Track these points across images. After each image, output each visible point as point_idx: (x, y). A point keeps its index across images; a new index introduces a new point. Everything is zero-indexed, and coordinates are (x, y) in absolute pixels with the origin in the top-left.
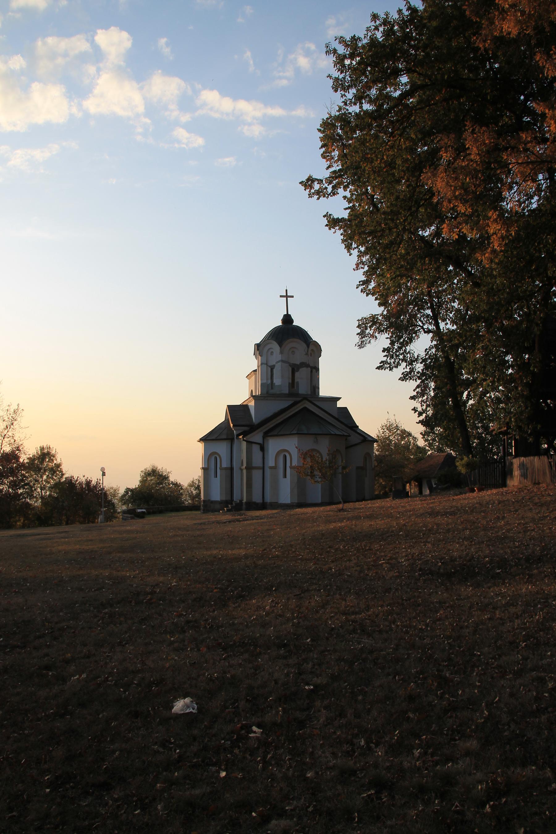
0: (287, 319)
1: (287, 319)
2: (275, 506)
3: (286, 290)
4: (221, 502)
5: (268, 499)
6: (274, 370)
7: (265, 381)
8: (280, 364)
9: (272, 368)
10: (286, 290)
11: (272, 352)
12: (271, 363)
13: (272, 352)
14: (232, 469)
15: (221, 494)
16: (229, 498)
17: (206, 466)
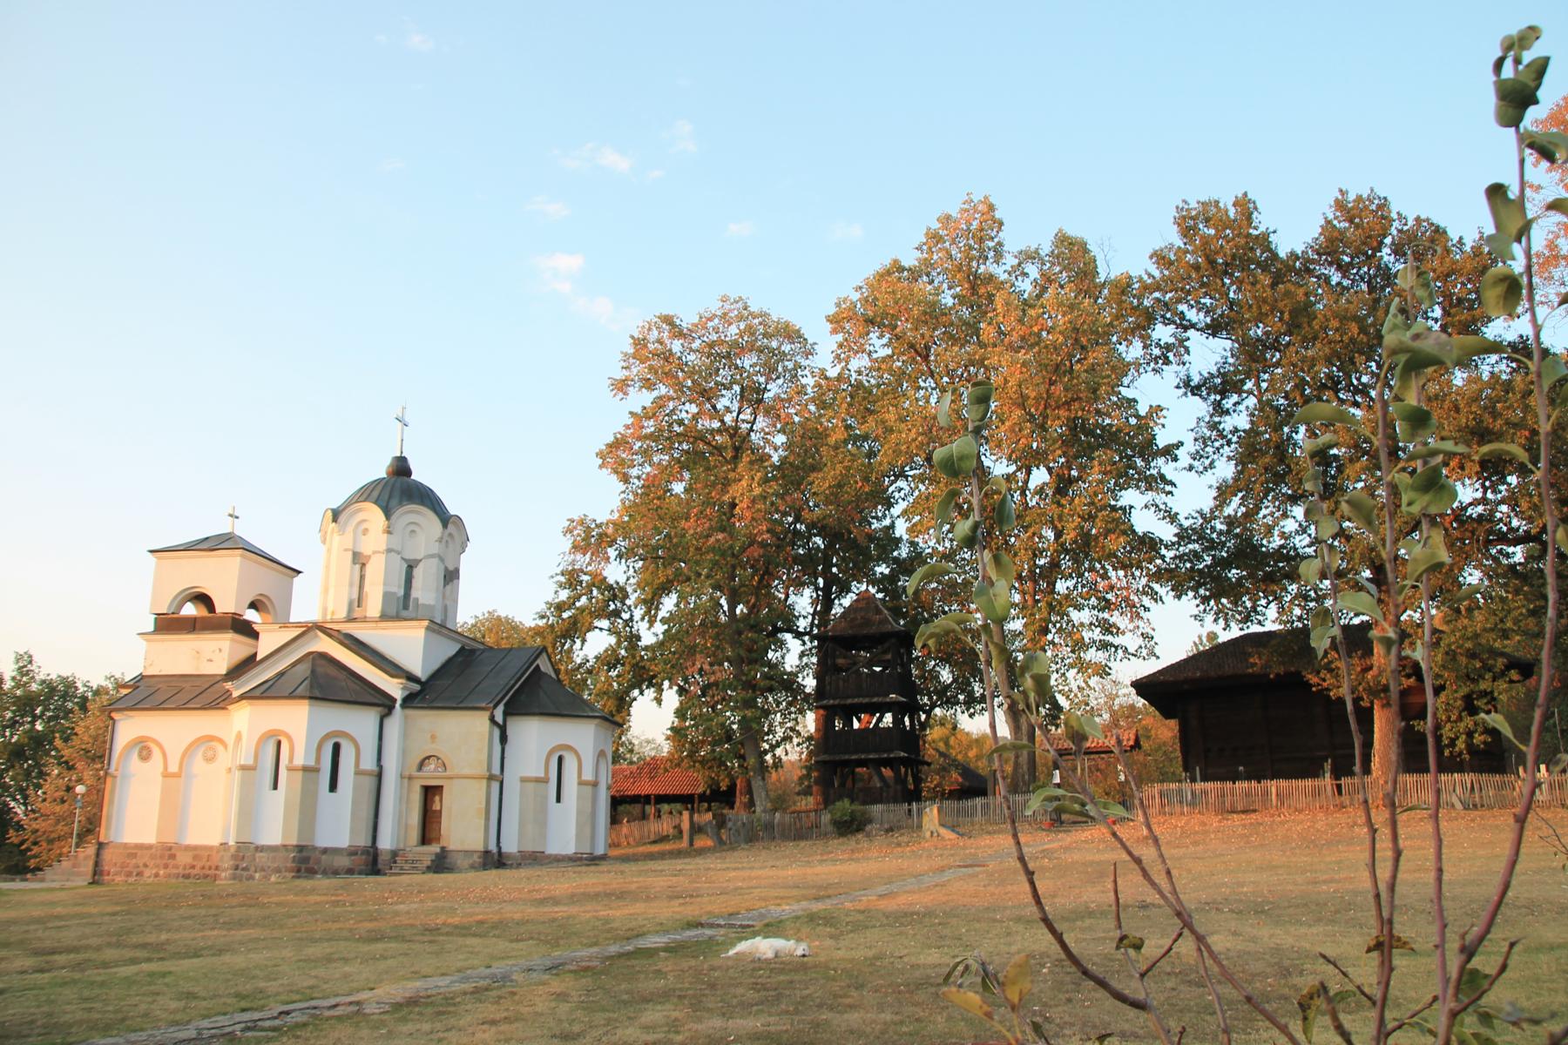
0: (401, 468)
1: (401, 468)
2: (535, 859)
3: (404, 408)
4: (352, 852)
5: (510, 846)
6: (418, 572)
7: (394, 589)
8: (436, 561)
9: (410, 568)
10: (404, 408)
11: (413, 531)
12: (412, 557)
13: (413, 531)
14: (380, 776)
15: (353, 831)
16: (363, 841)
17: (312, 763)
